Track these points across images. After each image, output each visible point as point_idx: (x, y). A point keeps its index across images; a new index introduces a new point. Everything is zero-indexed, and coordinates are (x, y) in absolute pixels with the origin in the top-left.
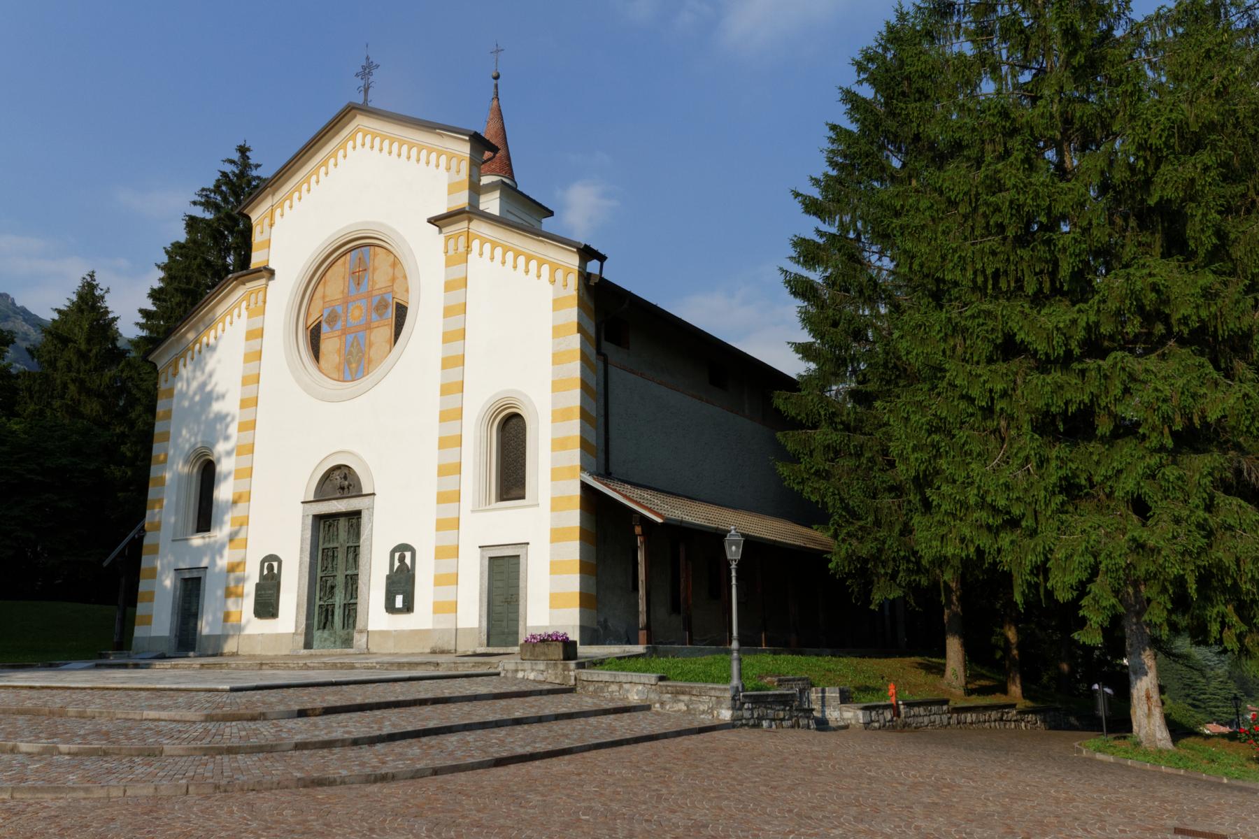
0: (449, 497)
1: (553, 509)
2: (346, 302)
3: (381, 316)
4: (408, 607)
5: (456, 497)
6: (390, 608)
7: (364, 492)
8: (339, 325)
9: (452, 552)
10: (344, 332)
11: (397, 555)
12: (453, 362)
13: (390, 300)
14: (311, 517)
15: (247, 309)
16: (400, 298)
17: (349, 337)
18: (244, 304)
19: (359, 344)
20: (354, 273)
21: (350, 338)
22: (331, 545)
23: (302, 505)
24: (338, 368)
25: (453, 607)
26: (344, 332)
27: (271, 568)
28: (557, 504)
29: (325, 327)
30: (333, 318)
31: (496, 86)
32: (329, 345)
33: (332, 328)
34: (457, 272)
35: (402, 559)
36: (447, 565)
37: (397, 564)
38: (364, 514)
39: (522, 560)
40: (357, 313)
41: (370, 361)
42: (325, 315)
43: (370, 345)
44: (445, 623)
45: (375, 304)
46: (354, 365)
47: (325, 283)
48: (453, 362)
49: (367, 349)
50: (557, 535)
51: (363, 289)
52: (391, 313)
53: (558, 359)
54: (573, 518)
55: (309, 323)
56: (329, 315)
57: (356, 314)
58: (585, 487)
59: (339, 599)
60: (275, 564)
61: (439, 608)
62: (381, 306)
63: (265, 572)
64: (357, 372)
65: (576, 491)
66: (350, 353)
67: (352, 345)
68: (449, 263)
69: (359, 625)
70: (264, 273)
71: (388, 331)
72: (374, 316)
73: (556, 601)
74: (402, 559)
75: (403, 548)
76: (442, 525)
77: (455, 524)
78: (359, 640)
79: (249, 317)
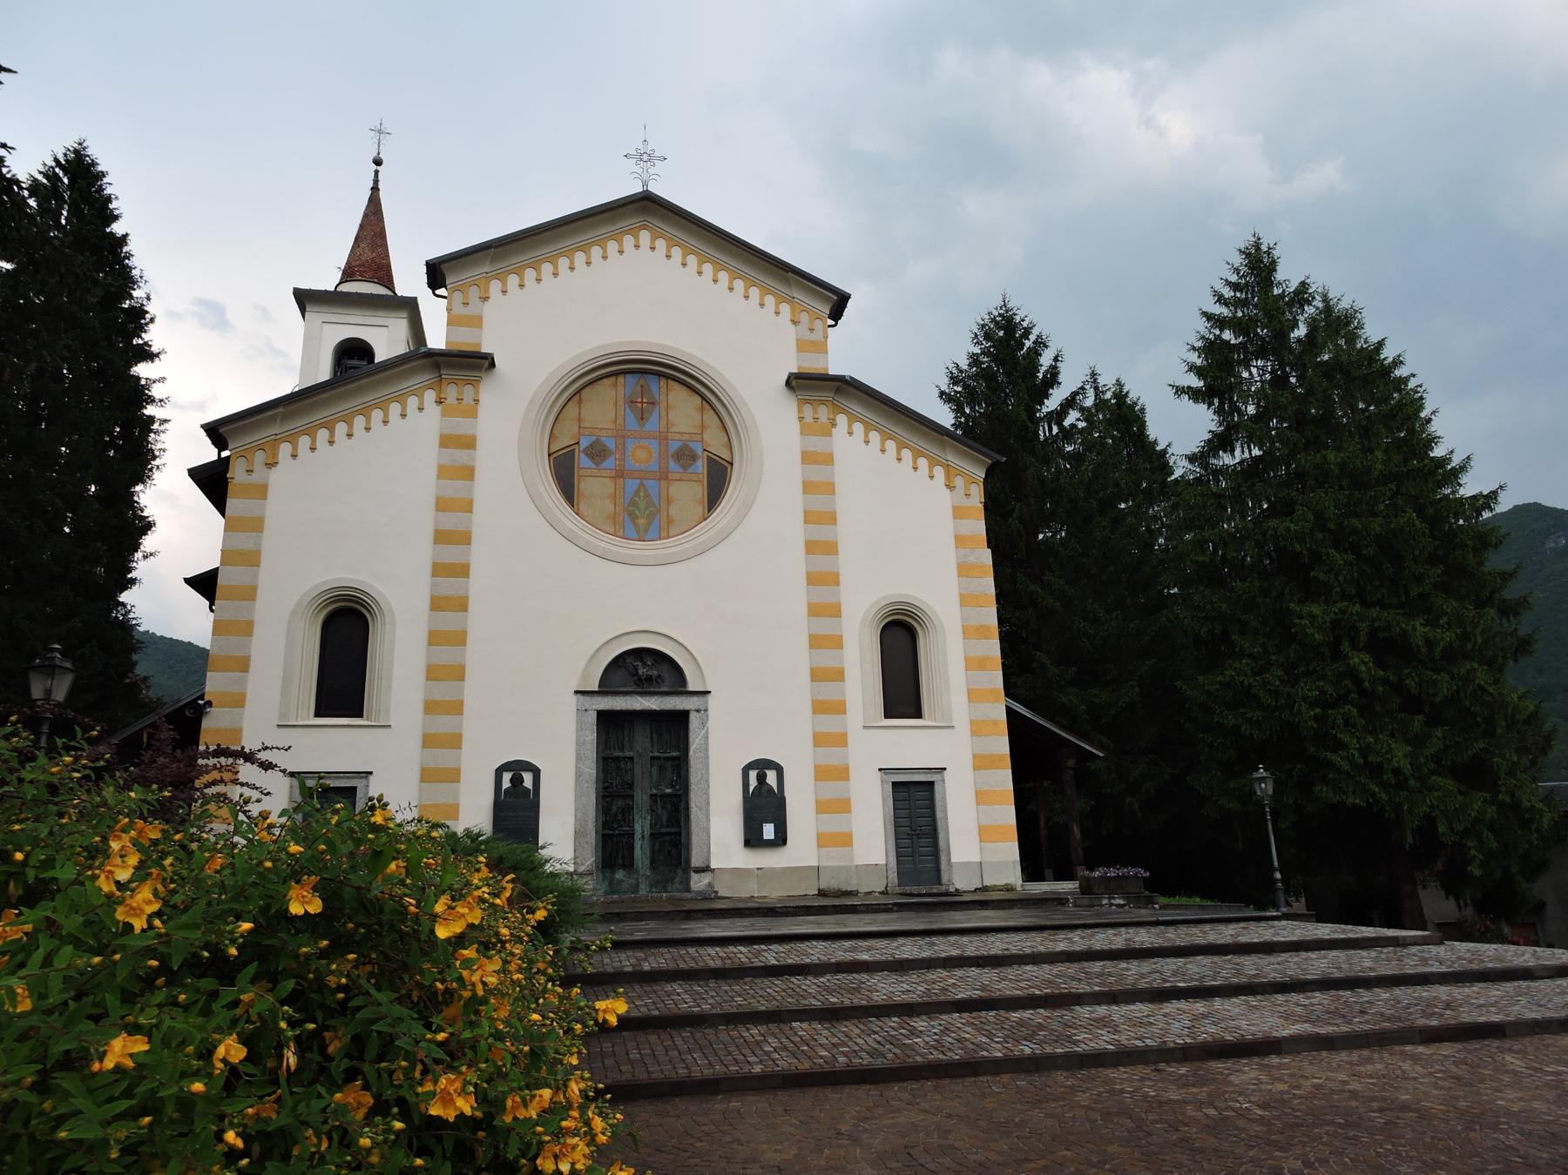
0: (828, 707)
1: (974, 733)
2: (622, 435)
3: (684, 467)
4: (781, 840)
5: (838, 708)
6: (753, 840)
7: (691, 687)
8: (610, 463)
9: (842, 773)
10: (620, 474)
11: (753, 774)
12: (821, 548)
13: (699, 451)
14: (594, 715)
15: (439, 402)
16: (726, 455)
17: (629, 482)
18: (430, 396)
19: (647, 495)
20: (632, 402)
21: (632, 485)
22: (617, 753)
23: (574, 698)
24: (613, 518)
25: (845, 840)
26: (620, 474)
27: (517, 781)
28: (977, 728)
29: (583, 461)
30: (597, 453)
31: (377, 172)
32: (594, 485)
33: (597, 465)
34: (817, 444)
35: (761, 779)
36: (832, 790)
37: (753, 783)
38: (693, 717)
39: (937, 787)
40: (642, 454)
41: (669, 522)
42: (584, 444)
43: (669, 501)
44: (833, 859)
45: (672, 450)
46: (642, 521)
47: (580, 402)
48: (821, 548)
49: (663, 506)
50: (981, 762)
51: (652, 424)
52: (701, 467)
53: (964, 570)
54: (1002, 745)
55: (554, 449)
56: (591, 445)
57: (642, 455)
58: (1010, 711)
59: (641, 826)
60: (528, 779)
61: (824, 840)
62: (685, 456)
63: (506, 784)
64: (646, 531)
65: (1002, 716)
66: (633, 503)
67: (637, 493)
68: (805, 430)
69: (696, 861)
70: (486, 363)
71: (699, 490)
72: (673, 465)
73: (986, 834)
74: (761, 779)
75: (762, 765)
76: (820, 740)
77: (840, 740)
78: (698, 882)
79: (443, 415)
